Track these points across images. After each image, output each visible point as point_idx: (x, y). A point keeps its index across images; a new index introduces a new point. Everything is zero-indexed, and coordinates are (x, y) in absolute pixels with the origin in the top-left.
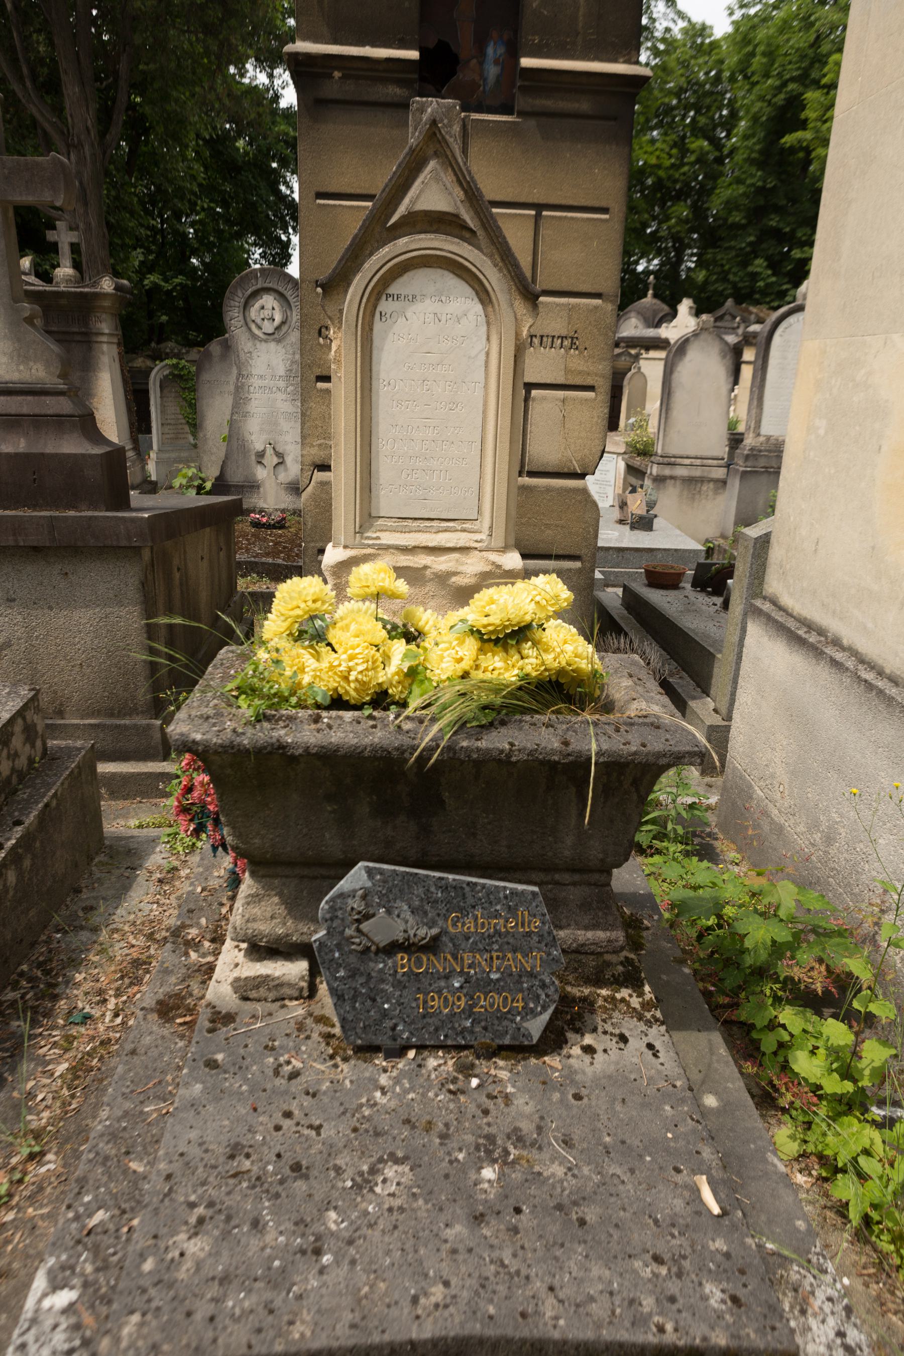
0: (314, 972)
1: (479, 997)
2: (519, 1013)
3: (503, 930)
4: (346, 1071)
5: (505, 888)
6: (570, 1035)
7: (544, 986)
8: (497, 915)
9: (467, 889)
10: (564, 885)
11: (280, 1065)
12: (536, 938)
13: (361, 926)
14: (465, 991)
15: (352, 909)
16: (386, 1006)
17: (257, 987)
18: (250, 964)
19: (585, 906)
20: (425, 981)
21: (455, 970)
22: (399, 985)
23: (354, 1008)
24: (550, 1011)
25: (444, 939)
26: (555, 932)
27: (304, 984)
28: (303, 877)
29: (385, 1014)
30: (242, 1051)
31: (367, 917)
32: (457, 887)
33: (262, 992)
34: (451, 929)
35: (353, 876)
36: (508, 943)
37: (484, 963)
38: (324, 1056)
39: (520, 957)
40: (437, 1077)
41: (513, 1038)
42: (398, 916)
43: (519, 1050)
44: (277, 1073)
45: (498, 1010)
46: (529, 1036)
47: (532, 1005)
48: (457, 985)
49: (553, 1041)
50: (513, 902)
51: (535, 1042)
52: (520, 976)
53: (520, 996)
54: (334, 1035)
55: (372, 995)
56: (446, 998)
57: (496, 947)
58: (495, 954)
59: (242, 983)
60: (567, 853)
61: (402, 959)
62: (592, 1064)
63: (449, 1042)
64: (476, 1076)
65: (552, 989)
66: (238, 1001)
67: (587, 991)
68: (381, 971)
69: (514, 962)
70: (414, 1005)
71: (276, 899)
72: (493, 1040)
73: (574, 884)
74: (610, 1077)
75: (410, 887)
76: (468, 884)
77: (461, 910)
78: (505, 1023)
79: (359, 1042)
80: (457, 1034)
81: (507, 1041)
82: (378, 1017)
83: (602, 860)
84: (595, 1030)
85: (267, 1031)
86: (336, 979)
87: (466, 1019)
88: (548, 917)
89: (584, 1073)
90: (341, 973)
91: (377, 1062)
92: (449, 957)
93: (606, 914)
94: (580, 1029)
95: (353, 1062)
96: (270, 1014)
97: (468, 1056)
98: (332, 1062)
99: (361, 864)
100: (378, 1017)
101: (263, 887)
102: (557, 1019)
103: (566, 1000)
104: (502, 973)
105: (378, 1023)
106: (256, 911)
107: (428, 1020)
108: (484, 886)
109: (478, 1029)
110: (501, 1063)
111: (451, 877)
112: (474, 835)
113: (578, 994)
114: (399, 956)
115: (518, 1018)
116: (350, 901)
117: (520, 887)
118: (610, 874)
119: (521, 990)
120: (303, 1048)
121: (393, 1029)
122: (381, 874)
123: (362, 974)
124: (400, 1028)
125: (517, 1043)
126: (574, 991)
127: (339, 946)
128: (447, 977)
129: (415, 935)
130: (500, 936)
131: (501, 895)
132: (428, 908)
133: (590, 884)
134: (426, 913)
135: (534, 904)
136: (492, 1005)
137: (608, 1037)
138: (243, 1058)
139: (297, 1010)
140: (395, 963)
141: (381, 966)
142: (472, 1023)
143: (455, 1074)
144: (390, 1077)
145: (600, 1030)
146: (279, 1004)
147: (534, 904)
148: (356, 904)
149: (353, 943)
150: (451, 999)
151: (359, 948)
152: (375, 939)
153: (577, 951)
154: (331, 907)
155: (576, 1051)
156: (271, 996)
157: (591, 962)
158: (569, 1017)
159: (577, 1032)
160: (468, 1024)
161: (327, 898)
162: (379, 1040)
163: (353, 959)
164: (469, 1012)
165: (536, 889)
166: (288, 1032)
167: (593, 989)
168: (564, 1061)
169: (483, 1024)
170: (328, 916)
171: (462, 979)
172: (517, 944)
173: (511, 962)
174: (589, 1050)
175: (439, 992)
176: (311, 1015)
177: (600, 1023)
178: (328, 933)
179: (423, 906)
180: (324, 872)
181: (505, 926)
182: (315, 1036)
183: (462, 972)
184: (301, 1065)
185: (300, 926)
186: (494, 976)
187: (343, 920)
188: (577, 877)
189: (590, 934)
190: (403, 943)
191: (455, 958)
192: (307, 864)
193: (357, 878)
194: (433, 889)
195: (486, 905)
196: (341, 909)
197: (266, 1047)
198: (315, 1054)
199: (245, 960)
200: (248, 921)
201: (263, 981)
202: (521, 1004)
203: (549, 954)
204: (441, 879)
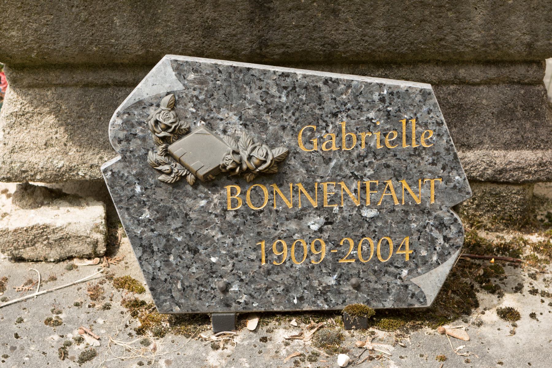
0: (111, 221)
1: (347, 243)
2: (406, 265)
3: (379, 147)
4: (160, 348)
5: (381, 86)
6: (482, 296)
7: (441, 225)
8: (370, 126)
9: (325, 89)
10: (474, 84)
11: (69, 344)
12: (428, 158)
13: (170, 148)
14: (326, 235)
15: (157, 122)
16: (213, 260)
17: (32, 243)
18: (22, 212)
19: (505, 114)
20: (268, 222)
21: (310, 206)
22: (233, 230)
23: (167, 263)
24: (451, 261)
25: (293, 162)
26: (460, 154)
27: (100, 237)
28: (87, 85)
29: (212, 271)
30: (15, 328)
31: (179, 133)
32: (311, 88)
33: (40, 250)
34: (302, 148)
35: (154, 76)
36: (388, 166)
37: (352, 195)
38: (128, 330)
39: (405, 185)
40: (288, 353)
41: (398, 299)
42: (225, 132)
43: (407, 316)
44: (64, 354)
45: (376, 261)
46: (420, 296)
47: (424, 253)
48: (315, 227)
49: (456, 301)
50: (393, 109)
51: (429, 304)
52: (406, 213)
53: (407, 240)
54: (143, 303)
55: (192, 244)
56: (298, 246)
57: (369, 172)
58: (368, 183)
59: (11, 238)
60: (476, 35)
61: (229, 191)
62: (513, 333)
63: (306, 307)
64: (344, 351)
65: (454, 229)
66: (7, 263)
67: (508, 237)
68: (203, 210)
69: (398, 192)
70: (253, 256)
71: (51, 119)
72: (368, 302)
73: (488, 83)
74: (538, 350)
75: (239, 89)
76: (326, 82)
77: (317, 119)
78: (386, 279)
79: (177, 310)
80: (316, 296)
81: (389, 304)
82: (202, 274)
83: (530, 45)
84: (519, 289)
85: (49, 300)
86: (139, 222)
87: (329, 274)
88: (445, 126)
89: (501, 345)
90: (147, 215)
91: (203, 335)
92: (301, 187)
93: (536, 125)
94: (497, 287)
95: (169, 337)
96: (54, 279)
97: (332, 326)
98: (141, 338)
99: (167, 58)
100: (202, 274)
101: (31, 102)
102: (464, 275)
103: (475, 250)
104: (380, 209)
105: (202, 283)
106: (23, 136)
107: (274, 277)
108: (349, 85)
109: (346, 288)
110: (381, 334)
111: (300, 72)
112: (335, 12)
113: (496, 242)
114: (228, 188)
115: (405, 272)
116: (152, 112)
117: (403, 85)
118: (541, 65)
119: (409, 233)
120: (100, 321)
121: (225, 290)
122: (196, 71)
123: (176, 216)
124: (235, 288)
125: (404, 306)
126: (491, 238)
127: (140, 177)
128: (299, 217)
129: (250, 158)
130: (375, 156)
131: (376, 97)
132: (267, 118)
133: (511, 82)
134: (264, 126)
135: (425, 109)
136: (366, 255)
137: (538, 297)
138: (17, 336)
139: (90, 271)
140: (223, 199)
141: (203, 203)
142: (338, 281)
143: (316, 350)
144: (222, 355)
145: (527, 288)
146: (64, 264)
147: (425, 109)
148: (166, 118)
149: (161, 172)
150: (306, 247)
151: (169, 179)
152: (193, 165)
153: (493, 181)
154: (126, 122)
155: (491, 316)
156: (54, 254)
157: (515, 195)
158: (481, 272)
159: (493, 292)
160: (332, 281)
161: (119, 109)
162: (203, 307)
163: (161, 194)
164: (333, 265)
165: (428, 87)
166: (78, 301)
167: (518, 234)
168: (473, 329)
169: (354, 281)
170: (122, 135)
171: (322, 220)
172: (400, 167)
173: (393, 193)
174: (509, 315)
175: (289, 238)
176: (111, 278)
177: (528, 280)
178: (124, 158)
179: (259, 117)
180: (117, 76)
181: (382, 142)
182: (117, 305)
183: (320, 209)
184: (98, 343)
185: (89, 155)
186: (368, 213)
187: (144, 139)
188: (492, 72)
189: (512, 155)
190: (233, 170)
191: (311, 190)
192: (91, 66)
193: (161, 79)
194: (273, 90)
195: (353, 112)
196: (140, 124)
197: (48, 321)
198: (118, 327)
199: (14, 207)
200: (12, 151)
201: (41, 233)
202: (408, 252)
203: (448, 180)
204: (283, 75)
